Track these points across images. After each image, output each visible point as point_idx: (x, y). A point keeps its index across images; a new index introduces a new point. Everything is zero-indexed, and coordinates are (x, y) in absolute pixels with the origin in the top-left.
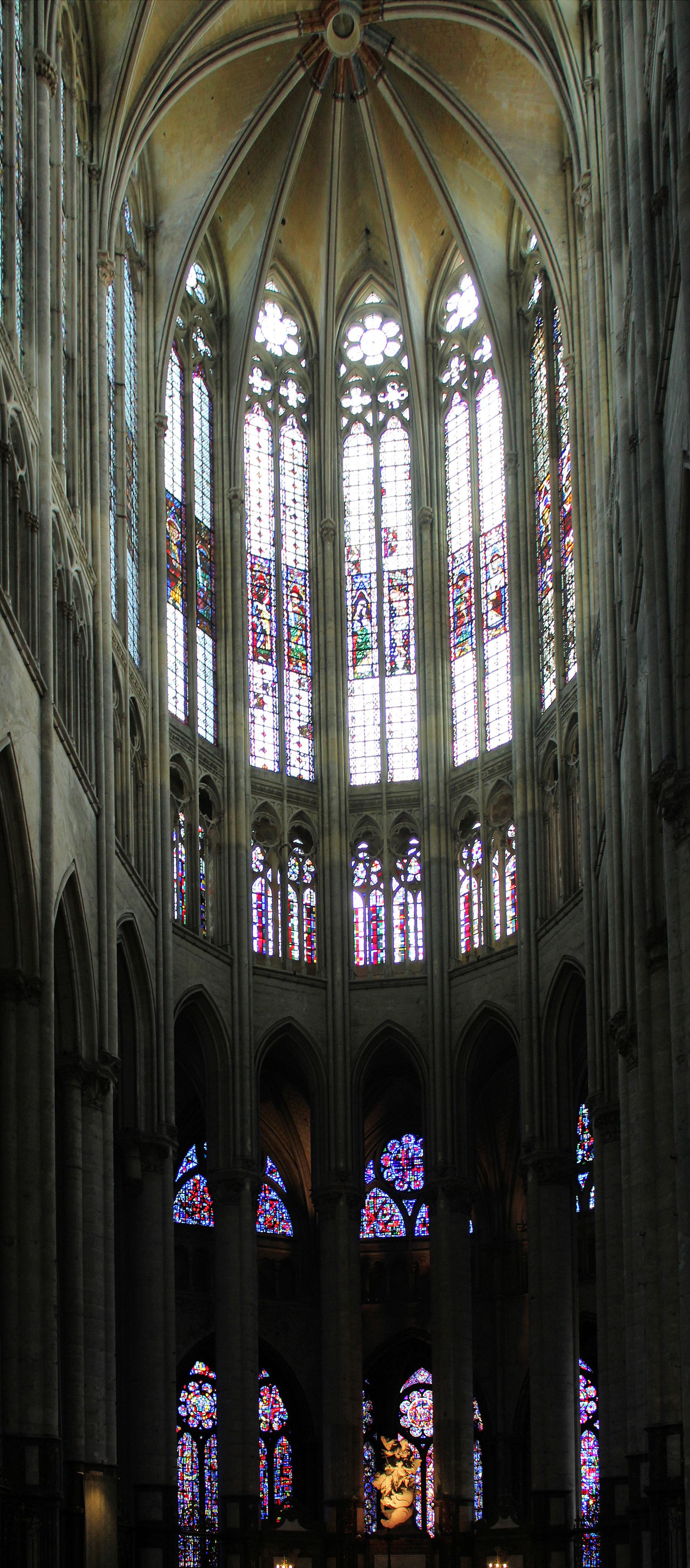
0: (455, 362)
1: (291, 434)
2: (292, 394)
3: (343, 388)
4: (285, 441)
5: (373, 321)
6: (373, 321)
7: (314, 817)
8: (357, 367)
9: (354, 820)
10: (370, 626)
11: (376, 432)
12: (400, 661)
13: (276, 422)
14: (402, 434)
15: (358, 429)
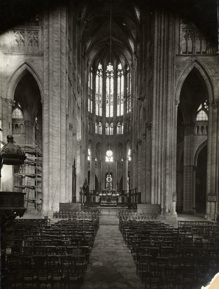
0: (119, 72)
1: (101, 78)
2: (101, 73)
3: (107, 73)
4: (100, 79)
5: (110, 66)
6: (110, 66)
7: (102, 120)
8: (108, 71)
9: (106, 120)
10: (109, 100)
11: (110, 78)
12: (111, 104)
13: (99, 76)
14: (113, 79)
15: (108, 78)
